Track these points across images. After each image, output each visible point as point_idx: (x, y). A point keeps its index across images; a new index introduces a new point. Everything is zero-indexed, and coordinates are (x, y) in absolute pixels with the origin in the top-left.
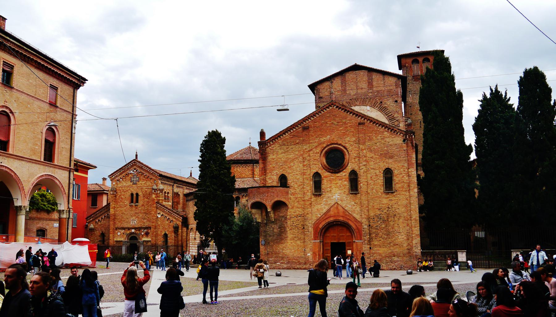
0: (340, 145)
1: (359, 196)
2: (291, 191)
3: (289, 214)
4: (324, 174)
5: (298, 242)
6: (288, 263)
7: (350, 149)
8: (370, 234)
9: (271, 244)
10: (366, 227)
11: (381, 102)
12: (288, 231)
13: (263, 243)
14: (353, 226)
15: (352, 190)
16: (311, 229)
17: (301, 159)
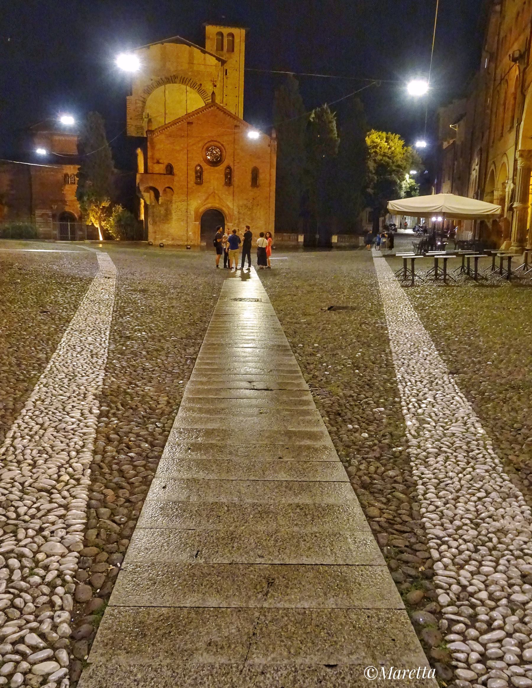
0: (219, 142)
1: (232, 187)
2: (176, 178)
3: (174, 198)
4: (206, 167)
5: (182, 223)
6: (173, 239)
7: (227, 147)
8: (239, 219)
9: (158, 223)
10: (236, 213)
11: (201, 85)
12: (174, 214)
13: (151, 222)
14: (226, 212)
15: (226, 183)
16: (193, 213)
17: (185, 151)
